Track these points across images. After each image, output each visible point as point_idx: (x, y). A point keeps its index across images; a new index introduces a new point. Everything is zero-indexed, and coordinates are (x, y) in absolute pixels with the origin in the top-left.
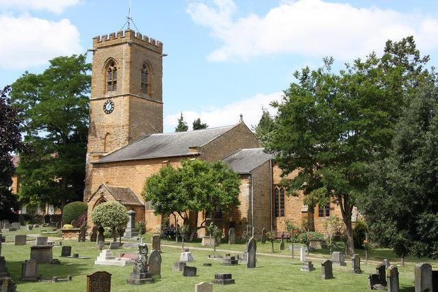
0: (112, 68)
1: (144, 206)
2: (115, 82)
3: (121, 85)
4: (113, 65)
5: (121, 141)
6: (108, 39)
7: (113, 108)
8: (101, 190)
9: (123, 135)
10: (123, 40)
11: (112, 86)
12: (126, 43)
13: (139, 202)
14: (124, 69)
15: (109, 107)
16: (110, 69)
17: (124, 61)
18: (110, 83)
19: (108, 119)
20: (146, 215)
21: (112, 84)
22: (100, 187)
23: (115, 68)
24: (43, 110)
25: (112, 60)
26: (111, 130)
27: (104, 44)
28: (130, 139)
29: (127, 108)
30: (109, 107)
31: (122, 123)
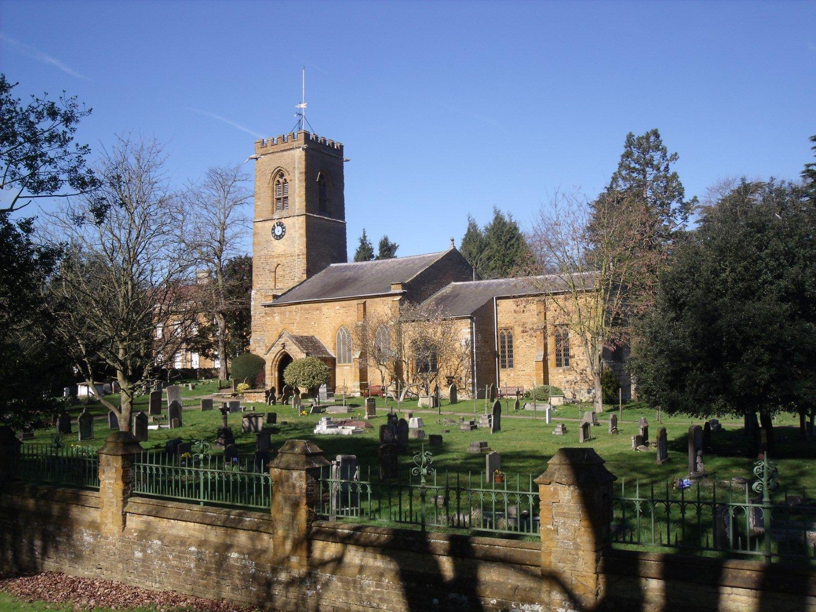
0: (281, 180)
1: (334, 359)
2: (287, 197)
3: (294, 203)
4: (282, 176)
5: (297, 275)
6: (275, 142)
7: (284, 232)
8: (282, 340)
9: (300, 265)
10: (295, 144)
11: (280, 204)
12: (299, 147)
13: (329, 354)
14: (297, 181)
15: (278, 231)
16: (278, 181)
17: (297, 172)
18: (279, 199)
19: (279, 247)
20: (338, 370)
21: (282, 201)
22: (280, 337)
23: (285, 180)
24: (538, 346)
25: (280, 170)
26: (282, 260)
27: (270, 149)
28: (311, 271)
29: (303, 231)
30: (278, 231)
31: (297, 252)
